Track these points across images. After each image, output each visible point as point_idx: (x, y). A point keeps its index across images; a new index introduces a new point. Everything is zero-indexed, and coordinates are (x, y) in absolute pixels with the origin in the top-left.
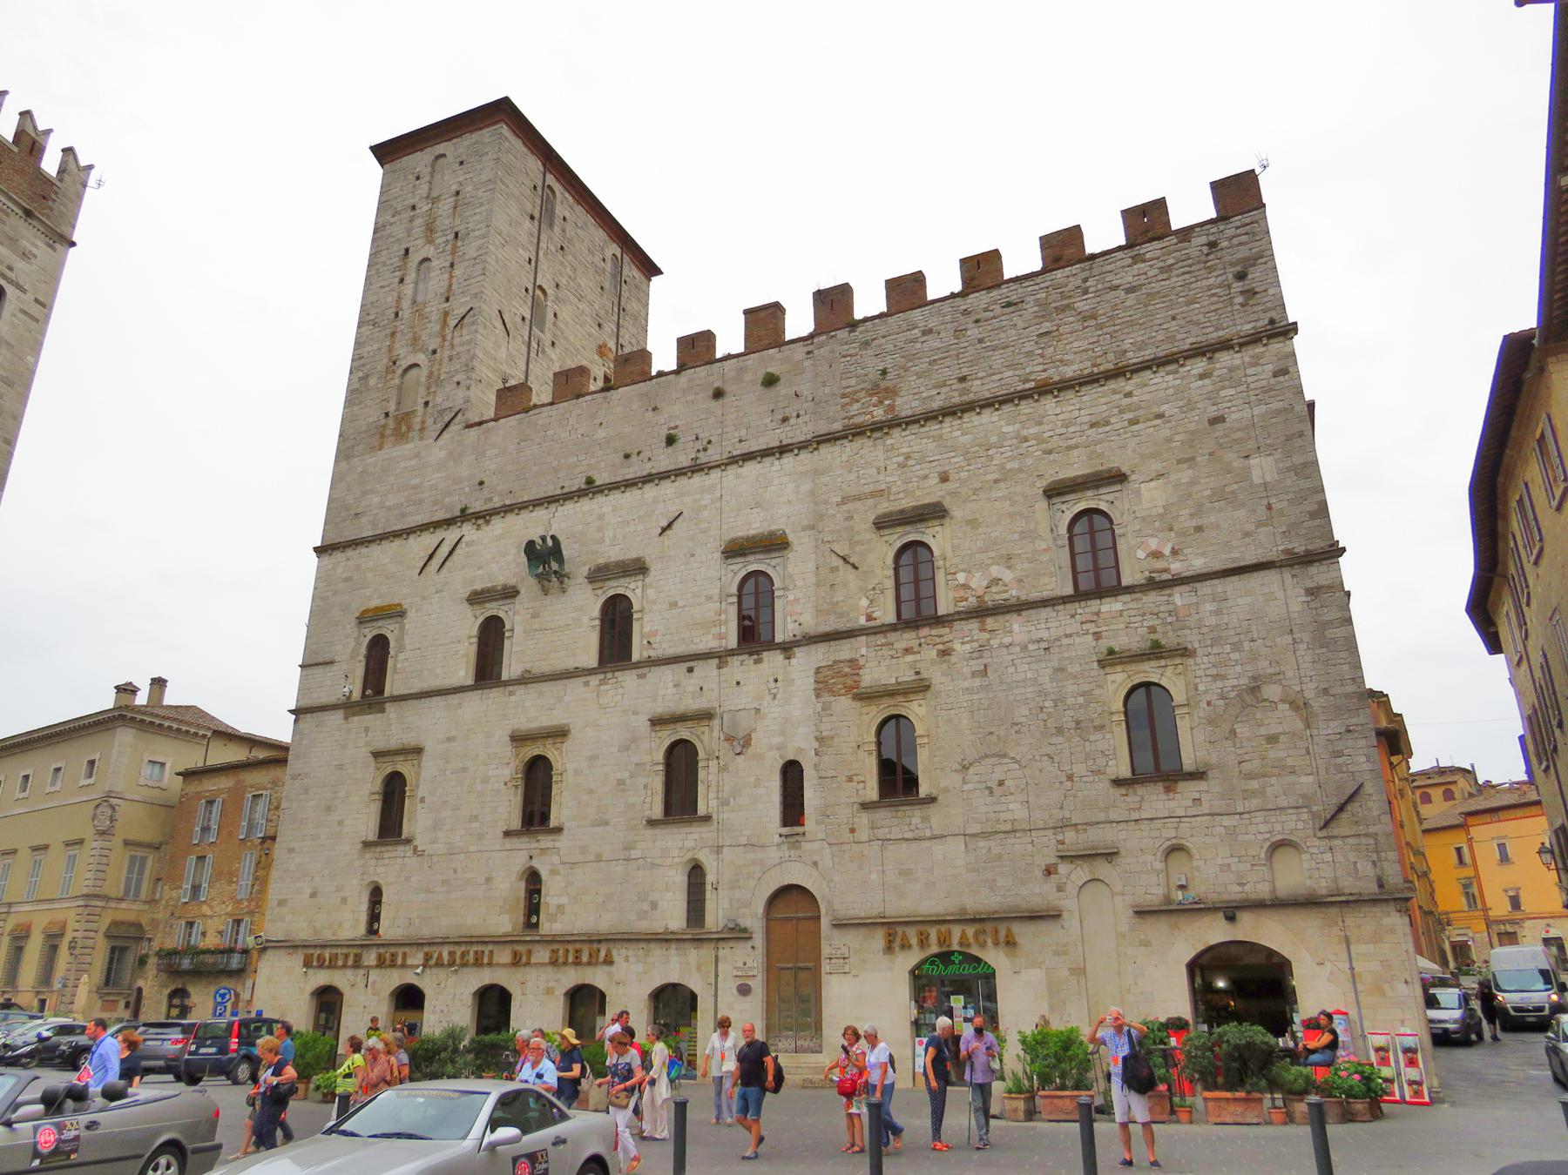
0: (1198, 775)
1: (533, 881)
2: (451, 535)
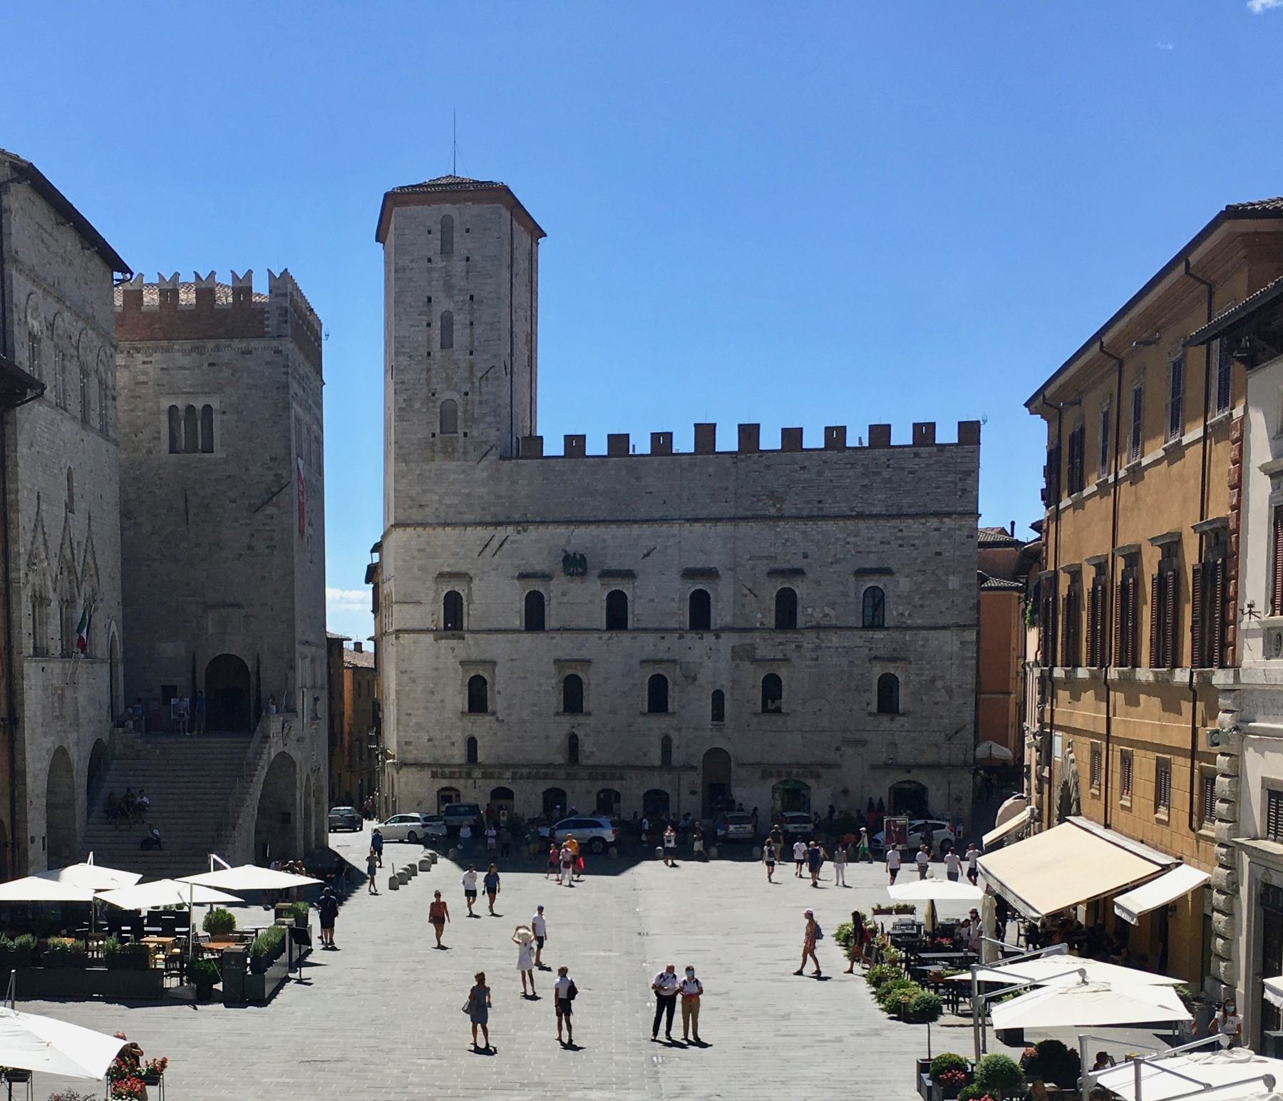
0: (903, 715)
1: (573, 741)
2: (501, 533)
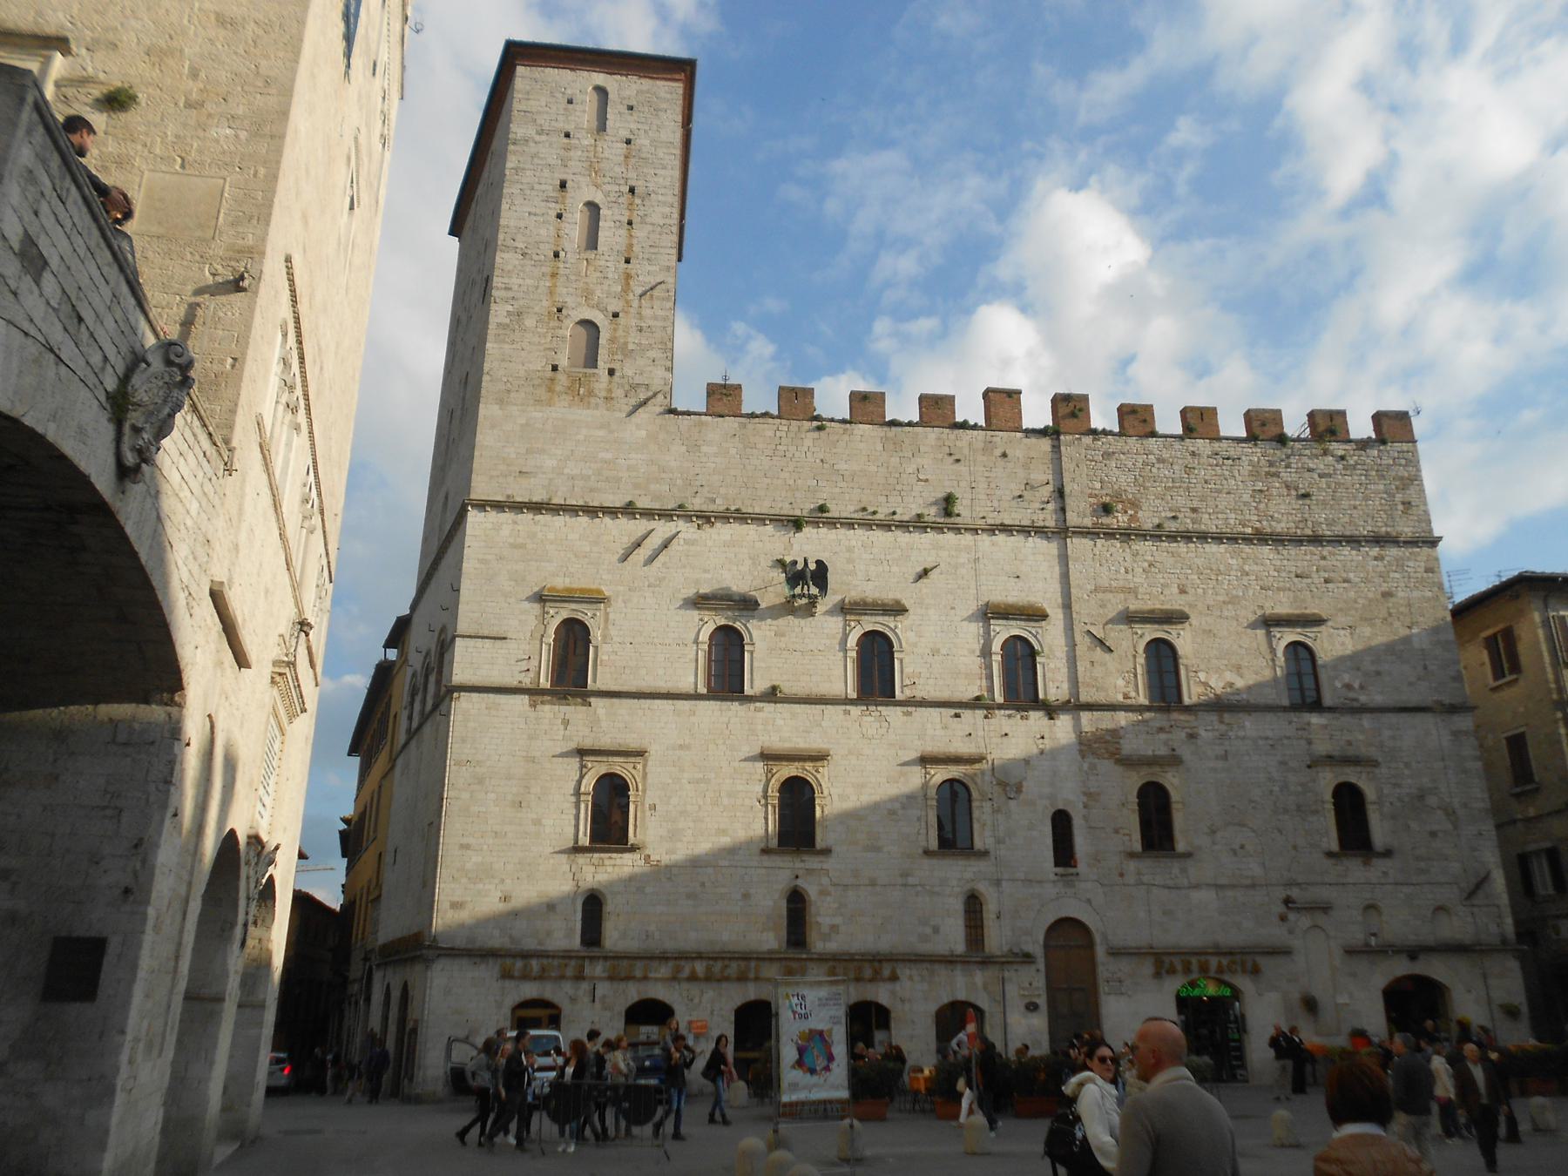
0: (1388, 853)
1: (797, 903)
2: (663, 529)
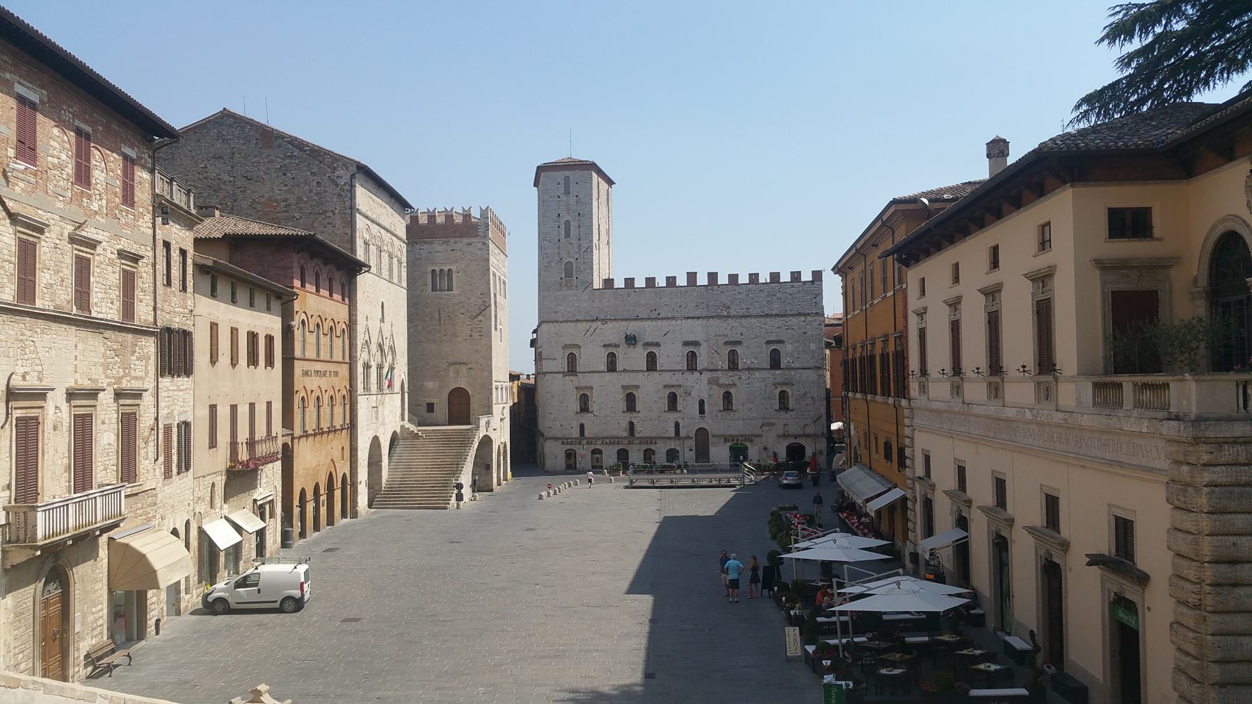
1: (631, 424)
2: (594, 325)
